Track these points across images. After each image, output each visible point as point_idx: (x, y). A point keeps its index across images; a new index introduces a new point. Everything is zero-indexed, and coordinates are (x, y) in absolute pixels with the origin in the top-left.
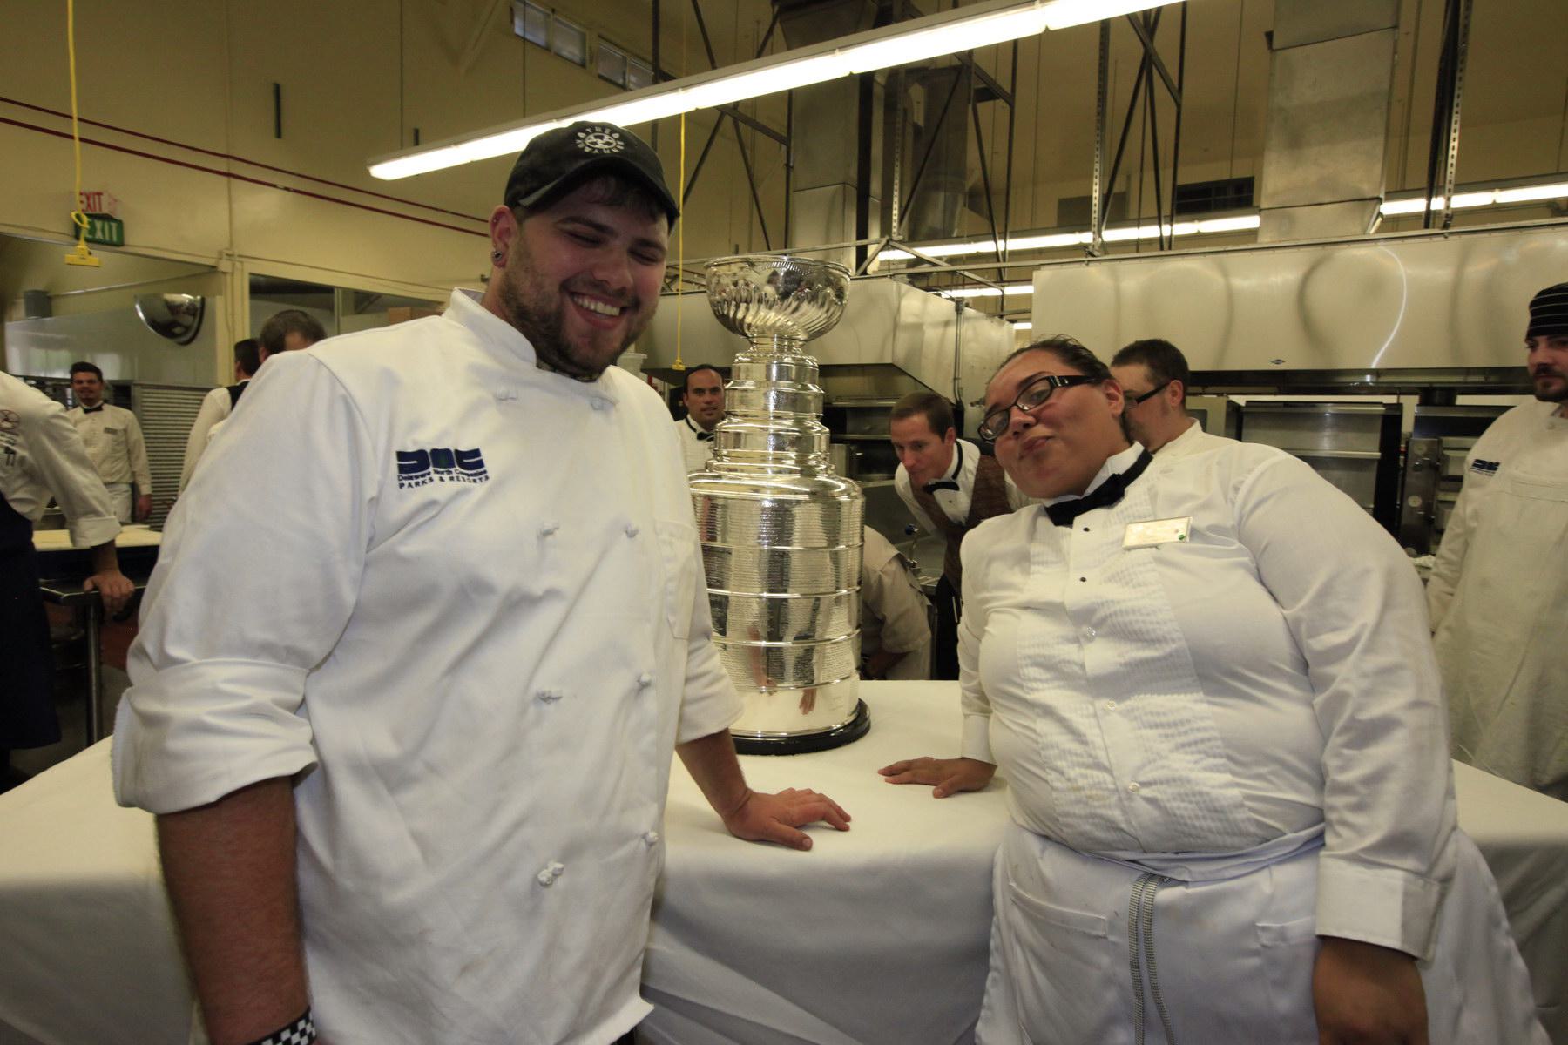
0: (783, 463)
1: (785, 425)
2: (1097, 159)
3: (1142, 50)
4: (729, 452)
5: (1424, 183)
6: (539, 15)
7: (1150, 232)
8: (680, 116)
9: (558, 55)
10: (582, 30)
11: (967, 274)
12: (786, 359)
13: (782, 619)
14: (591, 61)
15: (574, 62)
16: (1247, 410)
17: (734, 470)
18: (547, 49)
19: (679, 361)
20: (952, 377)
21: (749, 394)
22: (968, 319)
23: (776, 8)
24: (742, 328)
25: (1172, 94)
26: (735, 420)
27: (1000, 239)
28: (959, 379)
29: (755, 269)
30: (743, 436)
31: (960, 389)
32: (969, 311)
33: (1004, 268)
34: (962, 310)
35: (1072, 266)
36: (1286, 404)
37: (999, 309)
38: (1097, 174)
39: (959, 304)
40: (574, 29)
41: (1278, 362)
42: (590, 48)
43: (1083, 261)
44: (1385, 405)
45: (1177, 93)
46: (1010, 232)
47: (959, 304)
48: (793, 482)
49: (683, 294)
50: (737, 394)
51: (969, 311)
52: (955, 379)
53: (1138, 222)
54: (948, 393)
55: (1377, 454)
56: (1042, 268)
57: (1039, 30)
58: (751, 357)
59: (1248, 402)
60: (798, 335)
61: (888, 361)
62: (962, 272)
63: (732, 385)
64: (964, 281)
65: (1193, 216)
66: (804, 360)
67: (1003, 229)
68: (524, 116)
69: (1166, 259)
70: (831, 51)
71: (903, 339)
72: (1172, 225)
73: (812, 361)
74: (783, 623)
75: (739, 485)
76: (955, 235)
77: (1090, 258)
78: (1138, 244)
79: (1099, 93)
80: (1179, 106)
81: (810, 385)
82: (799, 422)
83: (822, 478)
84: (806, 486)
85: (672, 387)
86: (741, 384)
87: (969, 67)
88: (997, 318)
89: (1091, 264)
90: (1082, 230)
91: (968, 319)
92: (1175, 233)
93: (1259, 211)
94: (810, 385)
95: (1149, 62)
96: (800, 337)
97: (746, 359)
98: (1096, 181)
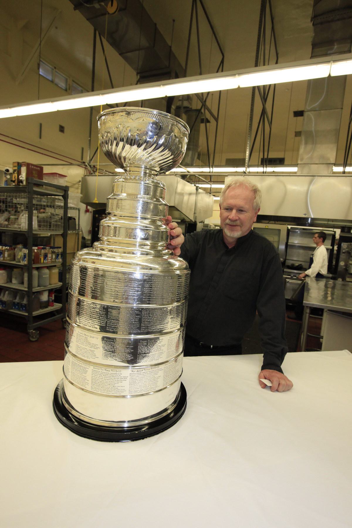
0: (142, 248)
1: (145, 223)
2: (248, 140)
3: (262, 107)
4: (107, 240)
5: (342, 162)
6: (50, 69)
7: (260, 169)
8: (100, 106)
9: (57, 85)
10: (67, 78)
11: (200, 177)
12: (148, 181)
13: (139, 351)
14: (69, 89)
15: (61, 88)
16: (291, 230)
17: (111, 251)
18: (52, 82)
19: (96, 199)
20: (194, 212)
21: (123, 202)
22: (200, 193)
23: (139, 77)
24: (120, 158)
25: (269, 123)
26: (113, 218)
27: (211, 167)
28: (196, 213)
29: (132, 116)
30: (118, 228)
31: (196, 217)
32: (200, 190)
33: (212, 175)
34: (198, 190)
35: (237, 176)
36: (304, 229)
37: (209, 191)
38: (248, 145)
39: (197, 188)
40: (63, 76)
41: (305, 214)
42: (69, 84)
43: (242, 175)
44: (333, 231)
45: (270, 123)
46: (215, 166)
47: (197, 187)
48: (147, 261)
49: (98, 176)
50: (115, 201)
51: (200, 190)
52: (194, 213)
53: (258, 166)
54: (192, 217)
55: (331, 247)
56: (228, 176)
57: (236, 87)
58: (125, 179)
59: (291, 227)
60: (155, 167)
61: (173, 205)
62: (199, 176)
63: (112, 196)
64: (199, 180)
65: (273, 166)
66: (159, 184)
67: (212, 165)
68: (39, 99)
69: (270, 177)
70: (159, 86)
71: (177, 197)
72: (266, 168)
73: (164, 185)
74: (139, 354)
75: (113, 262)
76: (194, 165)
77: (245, 174)
78: (257, 173)
79: (251, 117)
80: (271, 129)
81: (160, 199)
82: (153, 222)
83: (166, 257)
84: (159, 264)
85: (94, 210)
86: (118, 195)
87: (205, 106)
88: (209, 194)
89: (245, 176)
90: (237, 167)
91: (200, 193)
92: (267, 171)
93: (296, 165)
94: (160, 199)
95: (264, 112)
96: (156, 169)
97: (121, 180)
98: (248, 147)
